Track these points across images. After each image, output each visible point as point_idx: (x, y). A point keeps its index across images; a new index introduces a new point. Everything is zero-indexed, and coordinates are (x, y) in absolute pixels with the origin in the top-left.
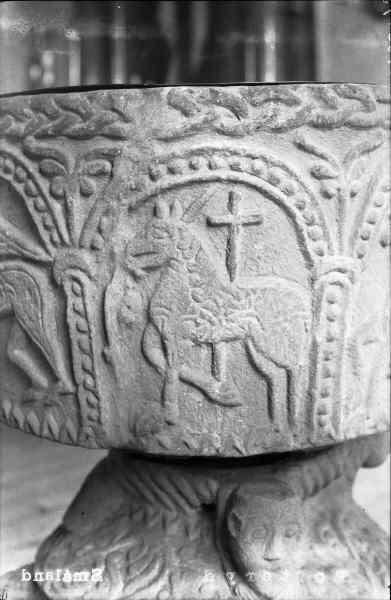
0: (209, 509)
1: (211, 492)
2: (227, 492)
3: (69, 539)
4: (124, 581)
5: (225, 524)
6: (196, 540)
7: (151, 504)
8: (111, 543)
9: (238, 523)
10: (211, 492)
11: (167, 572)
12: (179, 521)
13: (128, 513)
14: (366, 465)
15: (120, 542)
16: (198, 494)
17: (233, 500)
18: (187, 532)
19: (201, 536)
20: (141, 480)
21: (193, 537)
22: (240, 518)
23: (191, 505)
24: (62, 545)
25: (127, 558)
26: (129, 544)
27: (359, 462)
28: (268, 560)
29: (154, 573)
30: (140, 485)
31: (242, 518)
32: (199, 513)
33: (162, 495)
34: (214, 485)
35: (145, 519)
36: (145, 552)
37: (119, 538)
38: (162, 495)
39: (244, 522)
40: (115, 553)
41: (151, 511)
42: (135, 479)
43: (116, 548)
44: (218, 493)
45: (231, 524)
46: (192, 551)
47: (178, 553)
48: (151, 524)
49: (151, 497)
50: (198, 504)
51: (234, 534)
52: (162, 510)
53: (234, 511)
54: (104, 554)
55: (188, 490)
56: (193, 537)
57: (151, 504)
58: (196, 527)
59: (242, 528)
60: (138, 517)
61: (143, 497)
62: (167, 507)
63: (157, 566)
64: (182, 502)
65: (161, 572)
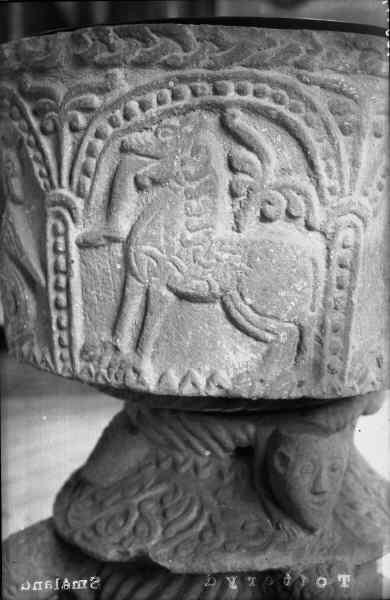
0: (243, 453)
1: (248, 435)
2: (267, 432)
3: (89, 491)
4: (163, 525)
5: (266, 468)
6: (231, 483)
7: (180, 451)
8: (142, 490)
9: (285, 459)
10: (248, 435)
11: (206, 514)
12: (211, 466)
13: (153, 462)
14: (365, 413)
15: (150, 489)
16: (234, 438)
17: (275, 441)
18: (220, 475)
19: (236, 478)
20: (171, 428)
21: (227, 480)
22: (287, 454)
23: (225, 449)
24: (84, 497)
25: (161, 502)
26: (161, 490)
27: (361, 411)
28: (315, 493)
29: (193, 515)
30: (170, 433)
31: (291, 455)
32: (231, 457)
33: (196, 443)
34: (251, 429)
35: (175, 466)
36: (180, 496)
37: (148, 485)
38: (196, 443)
39: (292, 459)
40: (149, 500)
41: (181, 458)
42: (166, 429)
43: (148, 494)
44: (256, 434)
45: (277, 463)
46: (229, 492)
47: (215, 494)
48: (183, 470)
49: (181, 445)
50: (230, 444)
51: (281, 470)
52: (193, 456)
53: (282, 449)
54: (136, 501)
55: (223, 435)
56: (227, 480)
57: (180, 451)
58: (230, 470)
59: (290, 465)
60: (166, 465)
61: (173, 446)
62: (199, 453)
63: (195, 509)
64: (215, 445)
65: (200, 513)
